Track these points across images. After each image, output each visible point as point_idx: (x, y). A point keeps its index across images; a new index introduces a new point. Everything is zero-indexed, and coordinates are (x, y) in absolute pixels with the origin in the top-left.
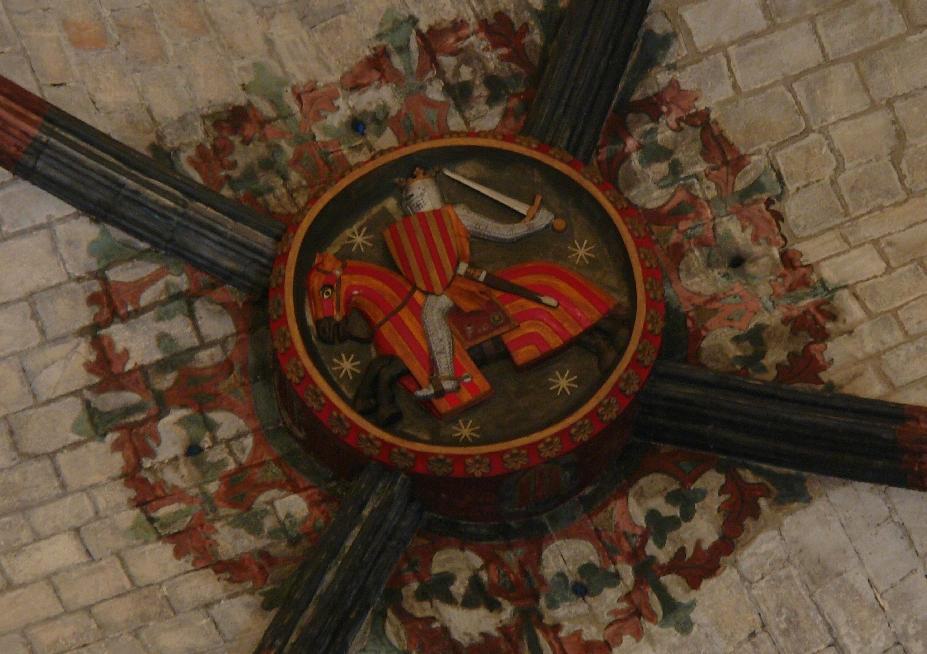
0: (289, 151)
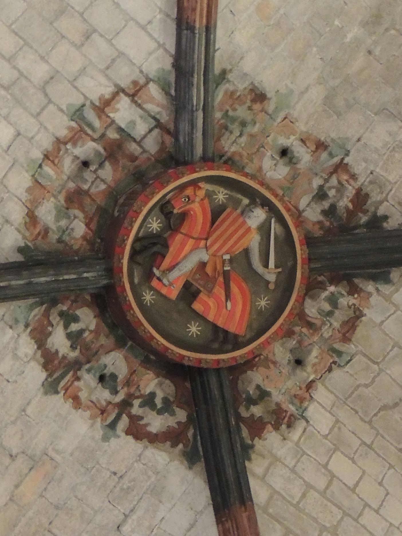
0: (256, 129)
